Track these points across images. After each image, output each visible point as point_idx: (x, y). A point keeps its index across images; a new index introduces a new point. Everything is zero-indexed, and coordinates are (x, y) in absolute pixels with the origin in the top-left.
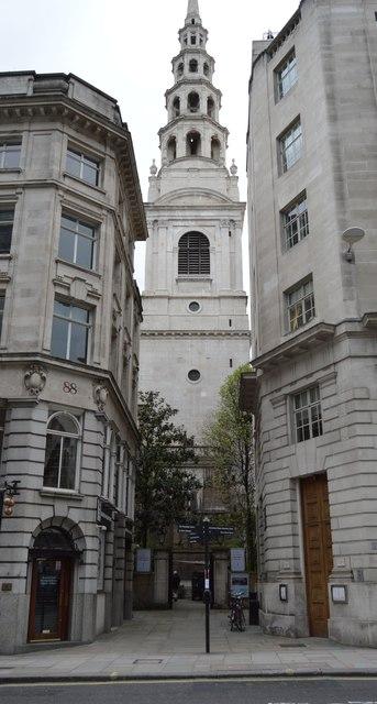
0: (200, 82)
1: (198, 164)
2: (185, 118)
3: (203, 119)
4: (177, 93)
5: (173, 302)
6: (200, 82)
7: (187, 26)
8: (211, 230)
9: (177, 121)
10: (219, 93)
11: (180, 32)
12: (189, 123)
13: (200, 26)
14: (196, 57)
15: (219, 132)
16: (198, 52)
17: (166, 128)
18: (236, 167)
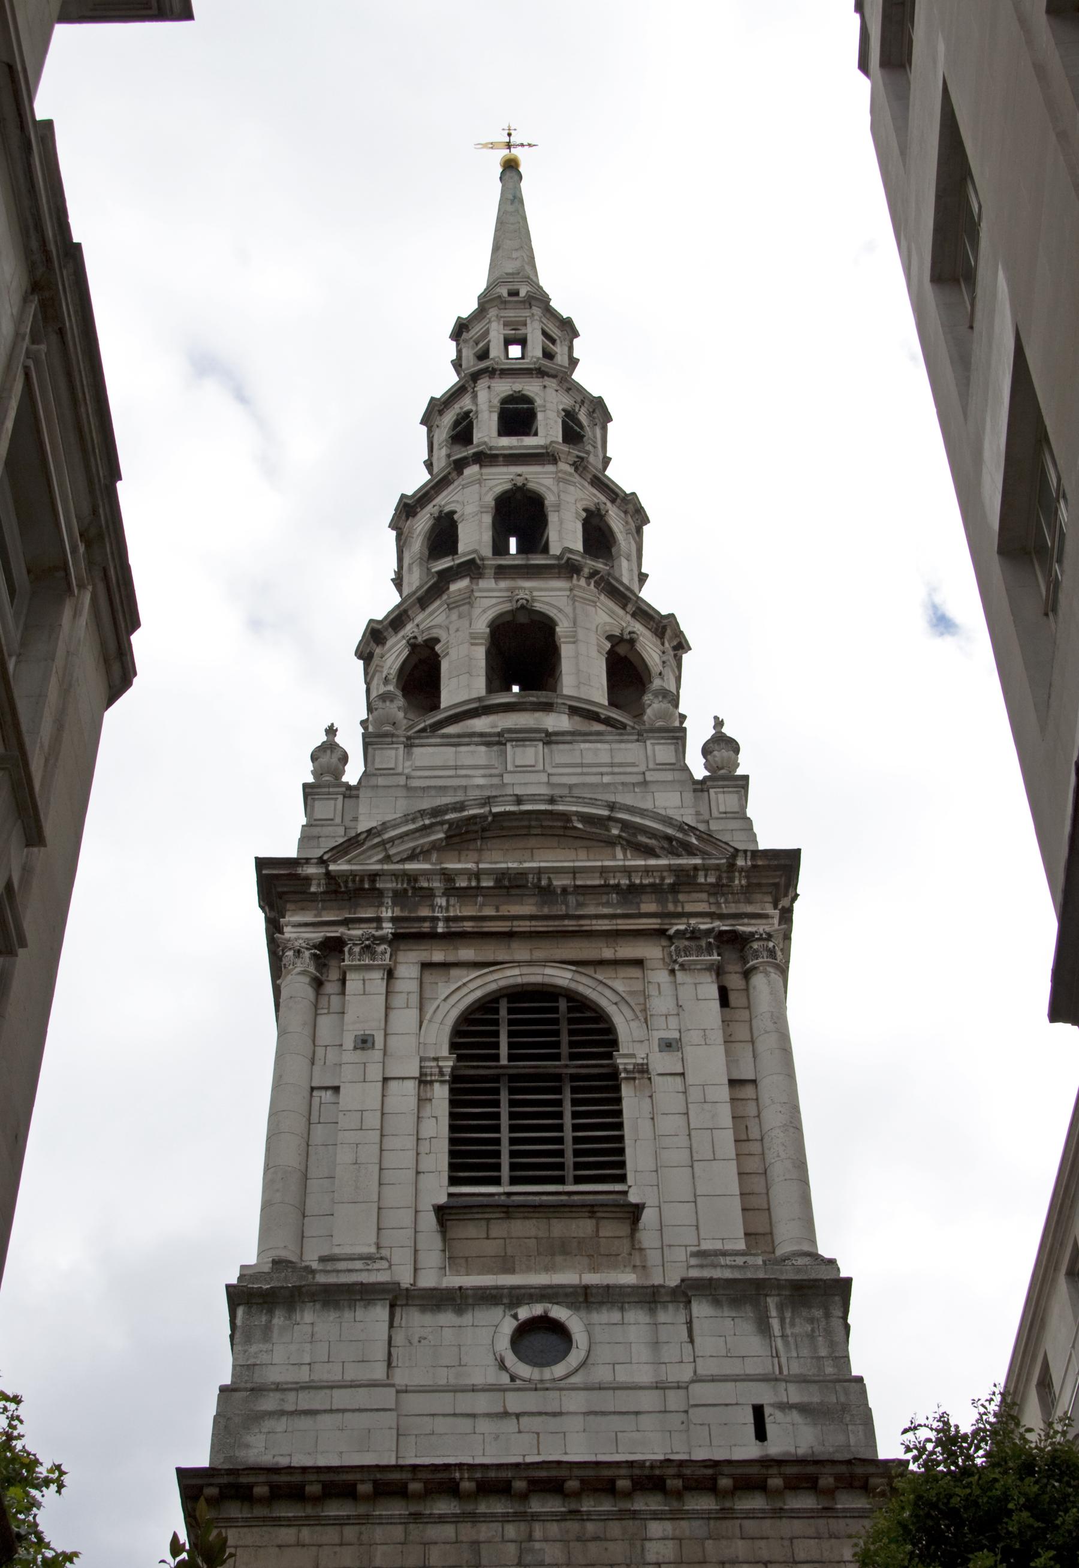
0: (544, 457)
1: (557, 722)
2: (472, 569)
3: (568, 568)
4: (444, 500)
5: (416, 1321)
6: (544, 457)
7: (486, 302)
8: (621, 982)
9: (445, 578)
10: (637, 516)
11: (460, 330)
12: (503, 584)
13: (540, 300)
14: (531, 387)
15: (638, 627)
16: (540, 373)
17: (397, 619)
18: (733, 746)
